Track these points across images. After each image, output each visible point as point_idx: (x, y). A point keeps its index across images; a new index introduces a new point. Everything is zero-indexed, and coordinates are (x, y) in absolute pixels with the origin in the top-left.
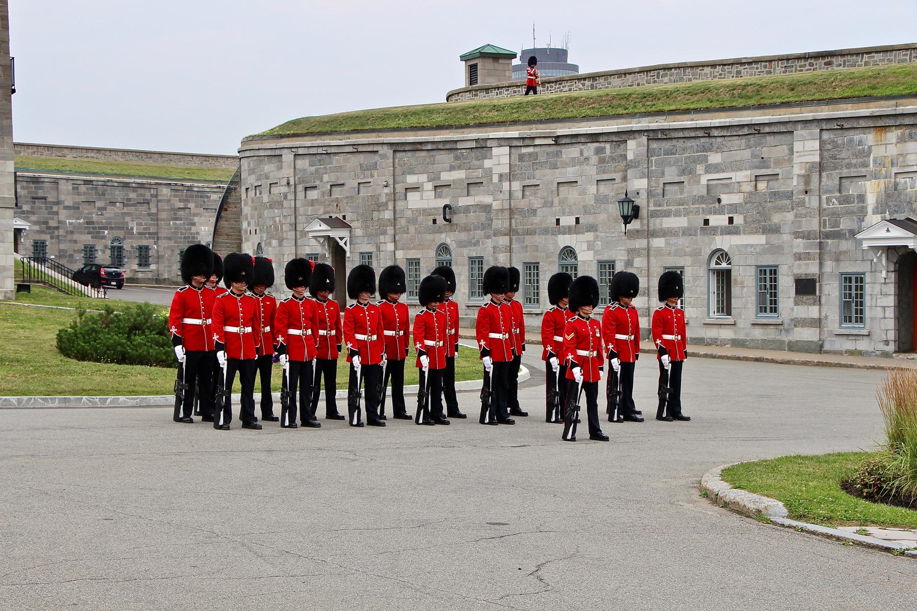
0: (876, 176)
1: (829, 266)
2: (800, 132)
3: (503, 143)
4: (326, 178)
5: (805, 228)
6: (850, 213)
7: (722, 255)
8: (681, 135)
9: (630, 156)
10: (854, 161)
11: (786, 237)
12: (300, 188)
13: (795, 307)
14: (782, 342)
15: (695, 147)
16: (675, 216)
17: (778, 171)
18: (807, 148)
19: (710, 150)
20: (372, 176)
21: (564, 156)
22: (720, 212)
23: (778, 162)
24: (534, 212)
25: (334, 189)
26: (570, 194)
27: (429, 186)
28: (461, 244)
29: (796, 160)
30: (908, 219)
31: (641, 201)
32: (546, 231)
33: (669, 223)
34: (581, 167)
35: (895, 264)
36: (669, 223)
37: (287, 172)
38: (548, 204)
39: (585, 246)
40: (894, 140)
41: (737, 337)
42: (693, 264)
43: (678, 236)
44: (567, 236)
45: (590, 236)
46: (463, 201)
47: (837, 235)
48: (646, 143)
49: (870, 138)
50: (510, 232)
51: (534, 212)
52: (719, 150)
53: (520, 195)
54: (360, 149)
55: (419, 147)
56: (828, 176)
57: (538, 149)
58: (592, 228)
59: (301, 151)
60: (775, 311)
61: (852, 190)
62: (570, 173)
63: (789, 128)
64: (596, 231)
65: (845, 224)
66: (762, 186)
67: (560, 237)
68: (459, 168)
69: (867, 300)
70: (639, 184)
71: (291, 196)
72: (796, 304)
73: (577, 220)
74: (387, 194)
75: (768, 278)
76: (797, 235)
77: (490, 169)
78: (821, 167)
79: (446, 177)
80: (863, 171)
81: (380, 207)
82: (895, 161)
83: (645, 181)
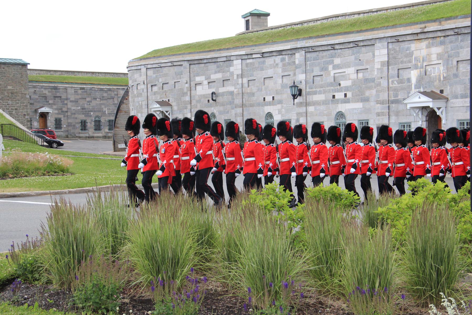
0: (416, 67)
3: (238, 57)
4: (160, 80)
5: (381, 99)
6: (403, 89)
8: (321, 49)
9: (297, 62)
10: (405, 60)
11: (372, 103)
12: (149, 86)
16: (319, 94)
17: (368, 67)
18: (381, 53)
20: (180, 78)
21: (266, 63)
23: (368, 62)
24: (253, 94)
25: (164, 86)
27: (206, 82)
28: (221, 113)
29: (376, 61)
30: (432, 91)
31: (302, 86)
32: (259, 105)
33: (316, 98)
34: (274, 68)
36: (316, 98)
37: (144, 78)
38: (260, 90)
39: (277, 112)
40: (424, 47)
43: (320, 105)
44: (269, 107)
45: (279, 106)
46: (221, 90)
47: (397, 102)
48: (304, 55)
49: (413, 46)
50: (243, 106)
51: (253, 94)
52: (339, 56)
53: (247, 85)
54: (175, 64)
55: (201, 62)
57: (254, 60)
58: (280, 102)
59: (149, 66)
62: (270, 72)
63: (372, 42)
64: (282, 103)
66: (360, 75)
67: (266, 107)
68: (219, 72)
70: (301, 77)
71: (145, 90)
73: (273, 97)
74: (187, 88)
76: (378, 102)
77: (233, 72)
79: (214, 77)
80: (409, 65)
81: (184, 94)
82: (425, 59)
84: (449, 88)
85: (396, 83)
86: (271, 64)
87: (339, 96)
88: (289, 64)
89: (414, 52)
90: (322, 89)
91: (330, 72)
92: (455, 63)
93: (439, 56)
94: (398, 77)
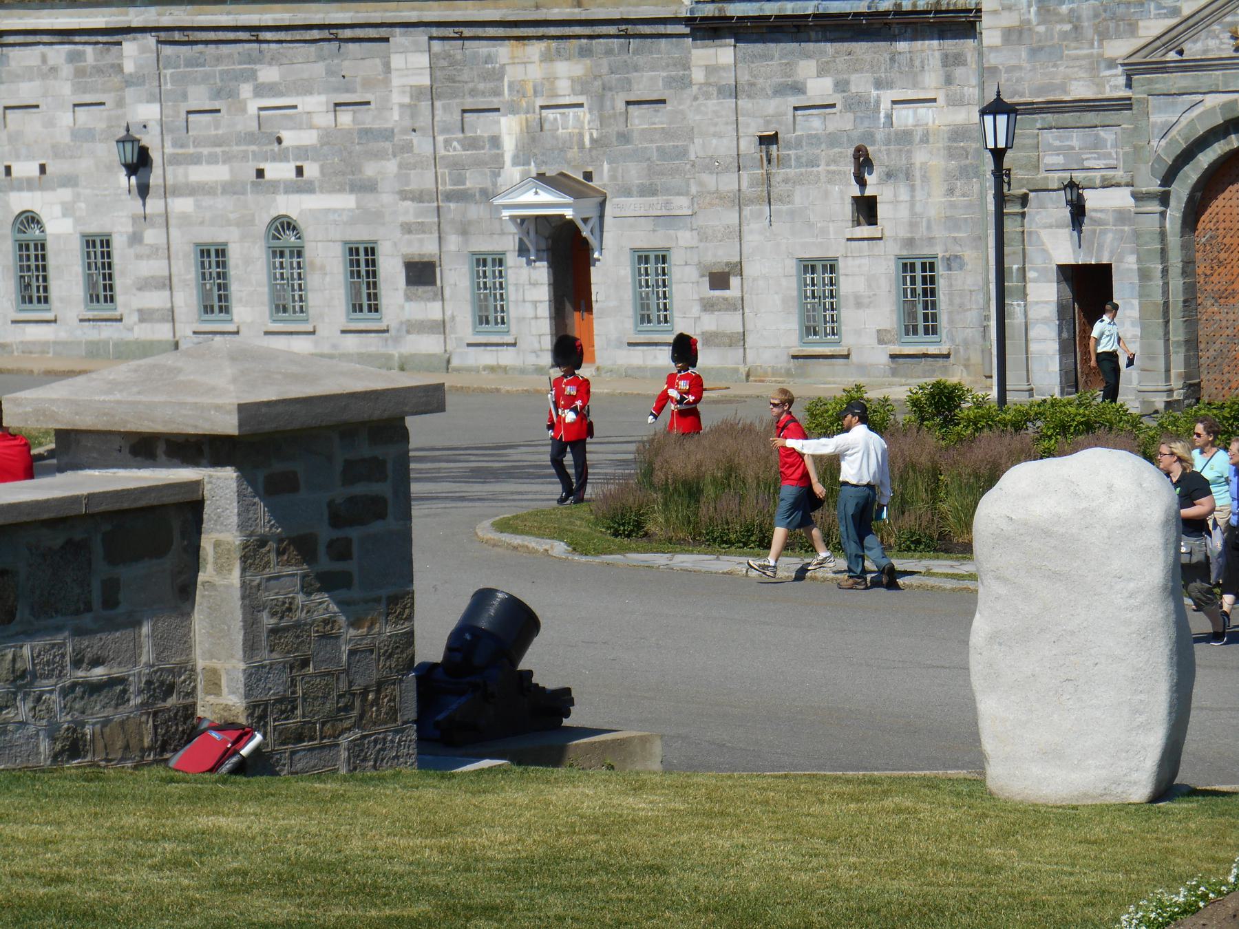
0: (513, 109)
1: (453, 242)
2: (399, 38)
5: (413, 186)
6: (478, 163)
7: (285, 225)
8: (212, 36)
9: (129, 67)
10: (481, 86)
11: (387, 198)
13: (407, 305)
14: (390, 357)
15: (236, 56)
16: (208, 163)
18: (410, 63)
19: (259, 61)
21: (13, 64)
22: (282, 157)
26: (29, 124)
29: (396, 81)
31: (150, 139)
33: (199, 174)
35: (547, 239)
36: (199, 174)
39: (57, 210)
40: (536, 58)
41: (318, 351)
42: (243, 238)
45: (66, 194)
49: (503, 52)
52: (273, 60)
56: (444, 108)
58: (69, 181)
60: (376, 310)
61: (481, 126)
62: (26, 91)
63: (383, 32)
65: (472, 181)
66: (346, 118)
69: (512, 293)
70: (145, 112)
72: (408, 298)
73: (43, 169)
75: (362, 261)
76: (404, 195)
78: (433, 94)
80: (495, 102)
82: (539, 88)
83: (155, 108)
84: (606, 166)
85: (458, 147)
86: (31, 68)
87: (280, 171)
88: (99, 71)
89: (508, 68)
90: (218, 150)
91: (244, 102)
92: (620, 106)
93: (581, 85)
94: (463, 131)
